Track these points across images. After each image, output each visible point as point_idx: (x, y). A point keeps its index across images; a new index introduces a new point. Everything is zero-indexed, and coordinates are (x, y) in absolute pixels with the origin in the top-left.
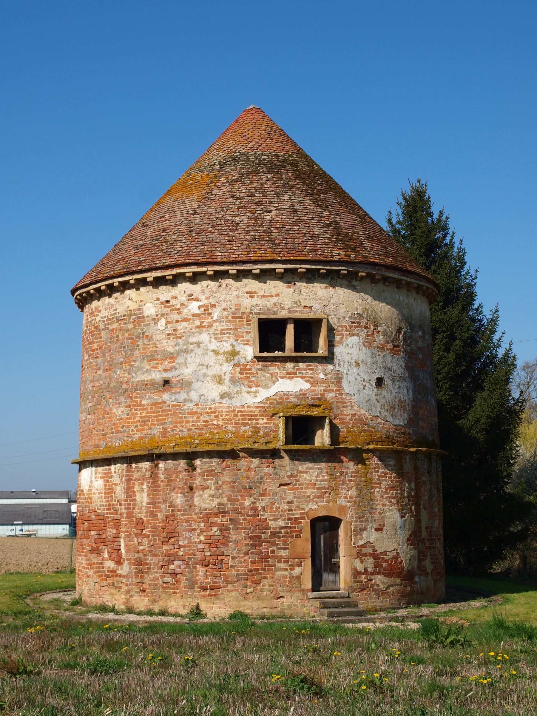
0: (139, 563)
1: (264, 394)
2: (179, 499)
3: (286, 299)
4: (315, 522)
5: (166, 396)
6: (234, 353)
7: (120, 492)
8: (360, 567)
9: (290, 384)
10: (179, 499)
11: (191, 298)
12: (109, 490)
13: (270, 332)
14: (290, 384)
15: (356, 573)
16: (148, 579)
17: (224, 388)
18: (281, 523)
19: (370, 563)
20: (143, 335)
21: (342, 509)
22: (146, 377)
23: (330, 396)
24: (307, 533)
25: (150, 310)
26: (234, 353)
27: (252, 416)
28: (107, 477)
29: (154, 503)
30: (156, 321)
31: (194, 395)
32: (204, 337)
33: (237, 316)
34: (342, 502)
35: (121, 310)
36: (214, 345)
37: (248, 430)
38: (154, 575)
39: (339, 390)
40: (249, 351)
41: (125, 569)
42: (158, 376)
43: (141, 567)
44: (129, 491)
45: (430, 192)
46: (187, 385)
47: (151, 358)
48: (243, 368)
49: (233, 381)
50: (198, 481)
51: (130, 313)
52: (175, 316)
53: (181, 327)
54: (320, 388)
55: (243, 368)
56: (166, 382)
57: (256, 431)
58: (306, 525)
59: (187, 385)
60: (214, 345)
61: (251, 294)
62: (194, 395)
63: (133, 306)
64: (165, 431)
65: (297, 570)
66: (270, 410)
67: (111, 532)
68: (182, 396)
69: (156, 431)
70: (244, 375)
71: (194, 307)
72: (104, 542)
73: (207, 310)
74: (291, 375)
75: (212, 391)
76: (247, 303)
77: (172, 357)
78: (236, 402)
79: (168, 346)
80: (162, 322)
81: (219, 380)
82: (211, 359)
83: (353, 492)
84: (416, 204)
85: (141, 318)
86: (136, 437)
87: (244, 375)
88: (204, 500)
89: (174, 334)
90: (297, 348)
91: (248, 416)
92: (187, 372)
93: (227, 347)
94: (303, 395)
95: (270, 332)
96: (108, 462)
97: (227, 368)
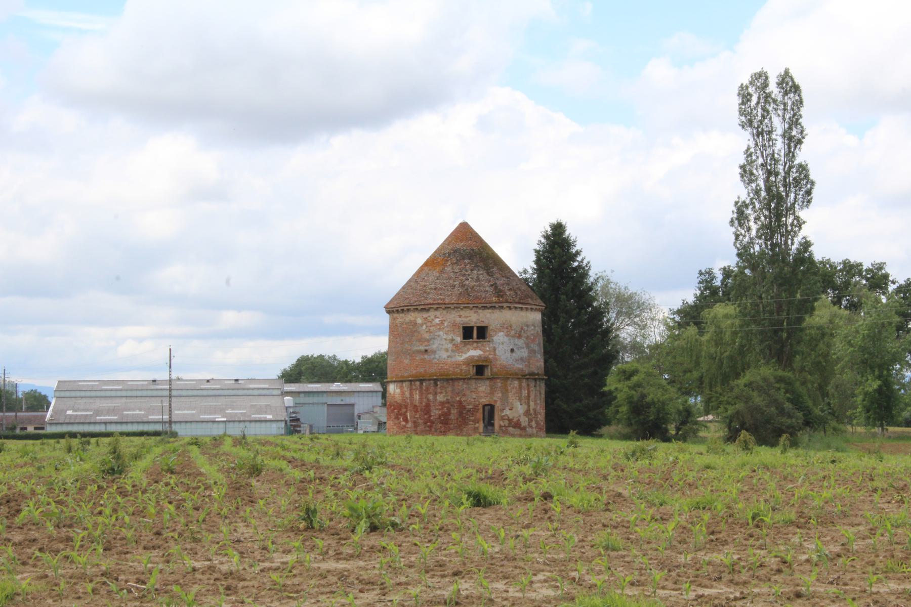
0: (415, 422)
1: (465, 356)
2: (431, 397)
3: (473, 318)
4: (484, 406)
5: (426, 356)
6: (453, 340)
7: (407, 394)
8: (502, 424)
9: (474, 352)
10: (431, 397)
11: (436, 317)
12: (403, 393)
13: (467, 333)
14: (474, 352)
15: (501, 426)
16: (419, 429)
17: (449, 354)
18: (471, 407)
19: (507, 423)
20: (416, 331)
21: (496, 401)
22: (418, 348)
23: (491, 356)
24: (481, 410)
25: (419, 321)
26: (453, 340)
27: (460, 365)
28: (401, 388)
29: (421, 399)
30: (422, 325)
31: (437, 356)
32: (441, 333)
33: (454, 325)
34: (495, 398)
35: (407, 320)
36: (445, 336)
37: (458, 370)
38: (421, 427)
39: (495, 354)
40: (459, 339)
41: (410, 425)
42: (422, 348)
43: (415, 424)
44: (411, 394)
45: (571, 232)
46: (434, 352)
47: (420, 341)
48: (456, 346)
49: (452, 351)
50: (439, 390)
51: (411, 322)
52: (429, 324)
53: (432, 329)
54: (487, 354)
55: (456, 346)
56: (426, 351)
57: (461, 370)
58: (481, 407)
59: (434, 352)
60: (445, 336)
61: (460, 316)
62: (437, 356)
63: (412, 319)
64: (425, 371)
65: (477, 425)
66: (468, 362)
67: (404, 410)
68: (432, 357)
69: (422, 370)
70: (457, 349)
71: (437, 321)
72: (401, 415)
73: (442, 322)
74: (475, 349)
75: (444, 355)
76: (458, 320)
77: (428, 341)
78: (453, 359)
79: (427, 336)
80: (424, 326)
81: (447, 350)
82: (444, 342)
83: (500, 395)
84: (557, 248)
85: (415, 324)
86: (414, 372)
87: (457, 349)
88: (440, 398)
89: (429, 332)
90: (478, 338)
91: (458, 365)
92: (434, 347)
93: (450, 337)
94: (480, 356)
95: (467, 333)
96: (402, 381)
97: (450, 346)
